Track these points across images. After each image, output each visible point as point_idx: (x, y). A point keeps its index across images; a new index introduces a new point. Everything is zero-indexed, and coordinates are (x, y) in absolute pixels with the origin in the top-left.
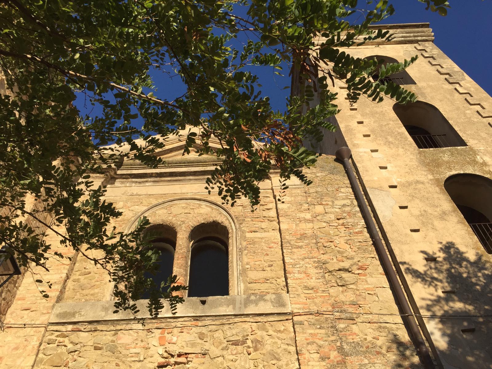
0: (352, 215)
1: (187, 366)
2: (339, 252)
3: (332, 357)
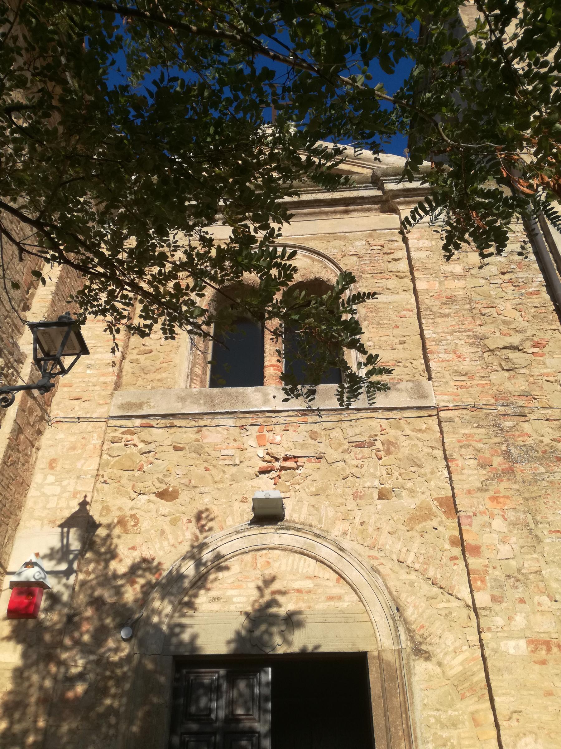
0: (524, 267)
1: (299, 472)
2: (504, 322)
3: (495, 464)
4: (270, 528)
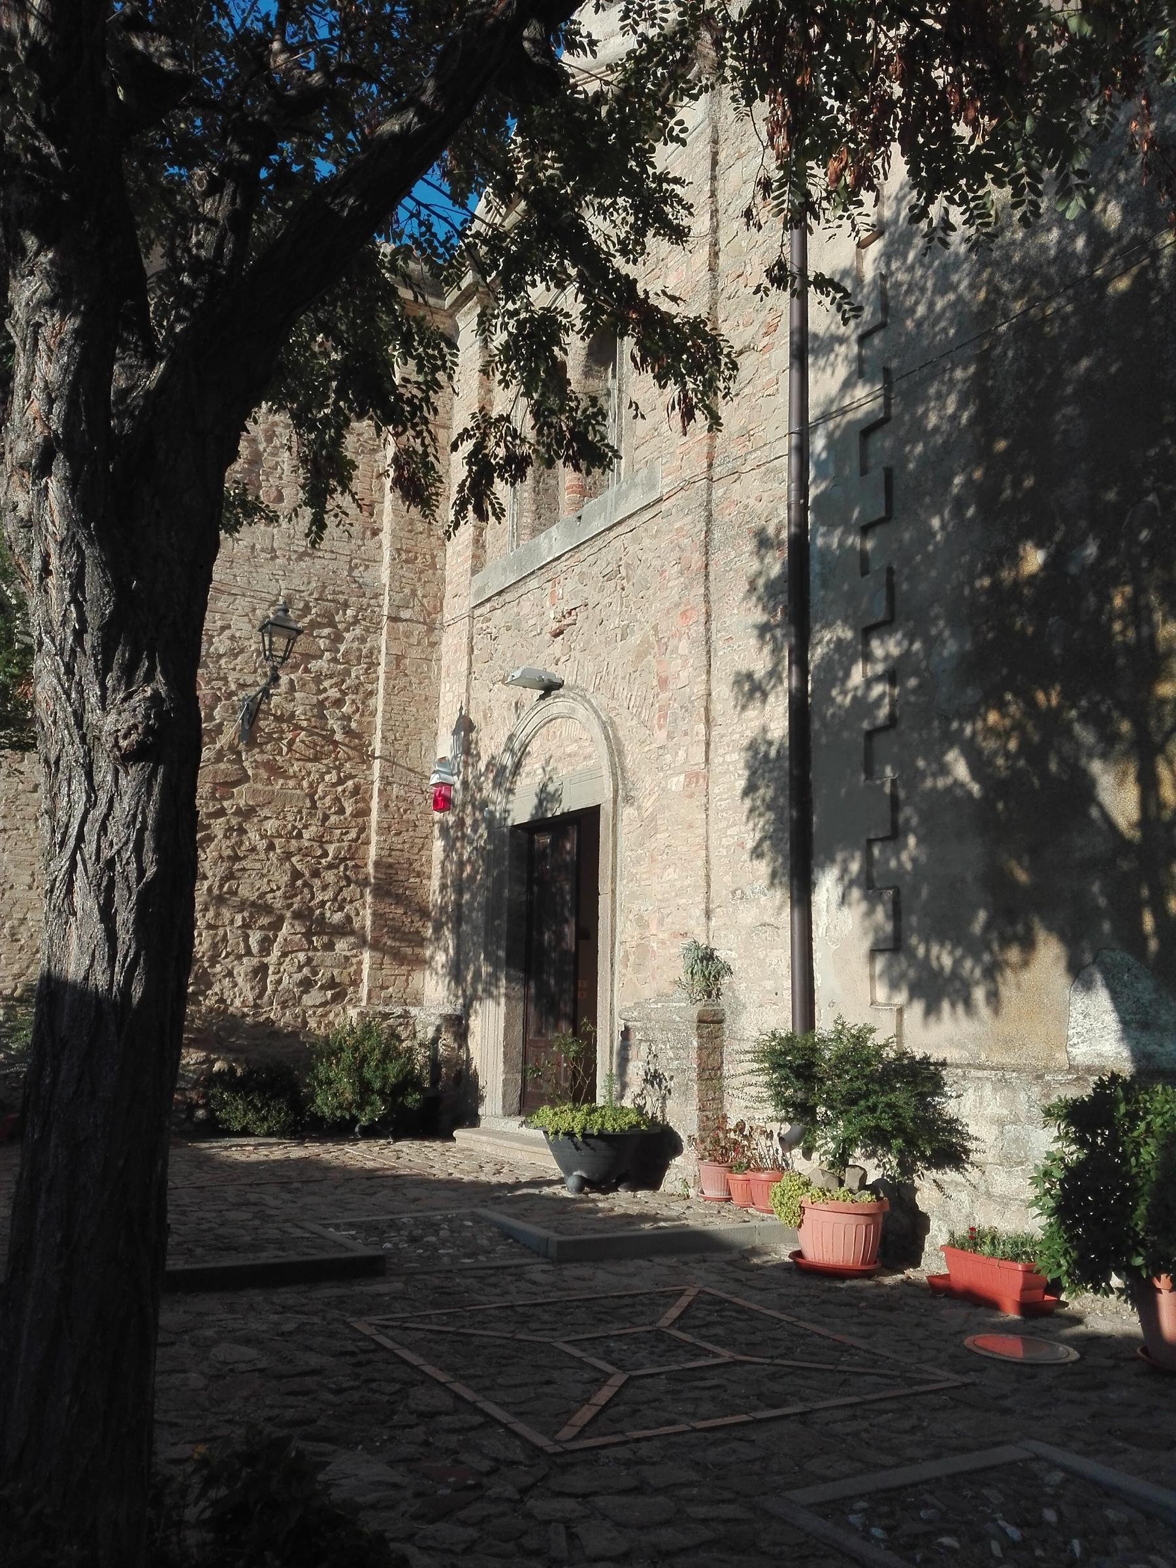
4: (549, 700)
